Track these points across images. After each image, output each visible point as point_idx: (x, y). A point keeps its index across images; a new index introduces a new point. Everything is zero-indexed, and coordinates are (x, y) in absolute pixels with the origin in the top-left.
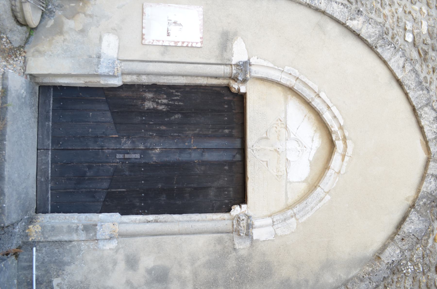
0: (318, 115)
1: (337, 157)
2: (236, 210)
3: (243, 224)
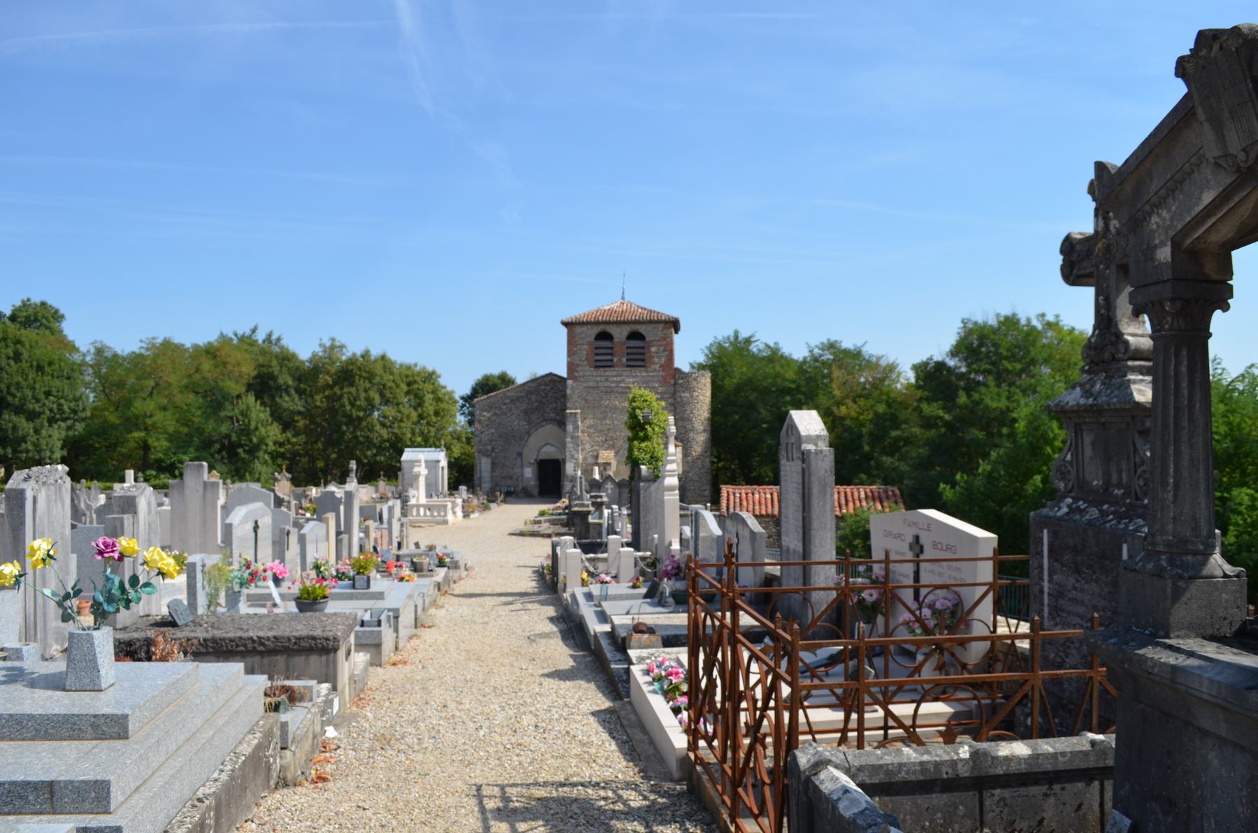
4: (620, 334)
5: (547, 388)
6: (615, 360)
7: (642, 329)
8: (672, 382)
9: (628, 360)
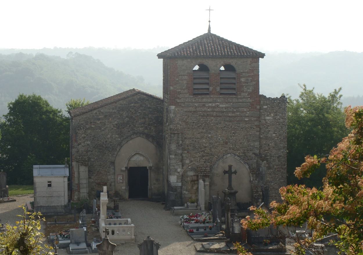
0: (133, 156)
1: (140, 153)
2: (148, 168)
3: (150, 168)
6: (211, 89)
7: (233, 62)
8: (258, 107)
9: (221, 89)
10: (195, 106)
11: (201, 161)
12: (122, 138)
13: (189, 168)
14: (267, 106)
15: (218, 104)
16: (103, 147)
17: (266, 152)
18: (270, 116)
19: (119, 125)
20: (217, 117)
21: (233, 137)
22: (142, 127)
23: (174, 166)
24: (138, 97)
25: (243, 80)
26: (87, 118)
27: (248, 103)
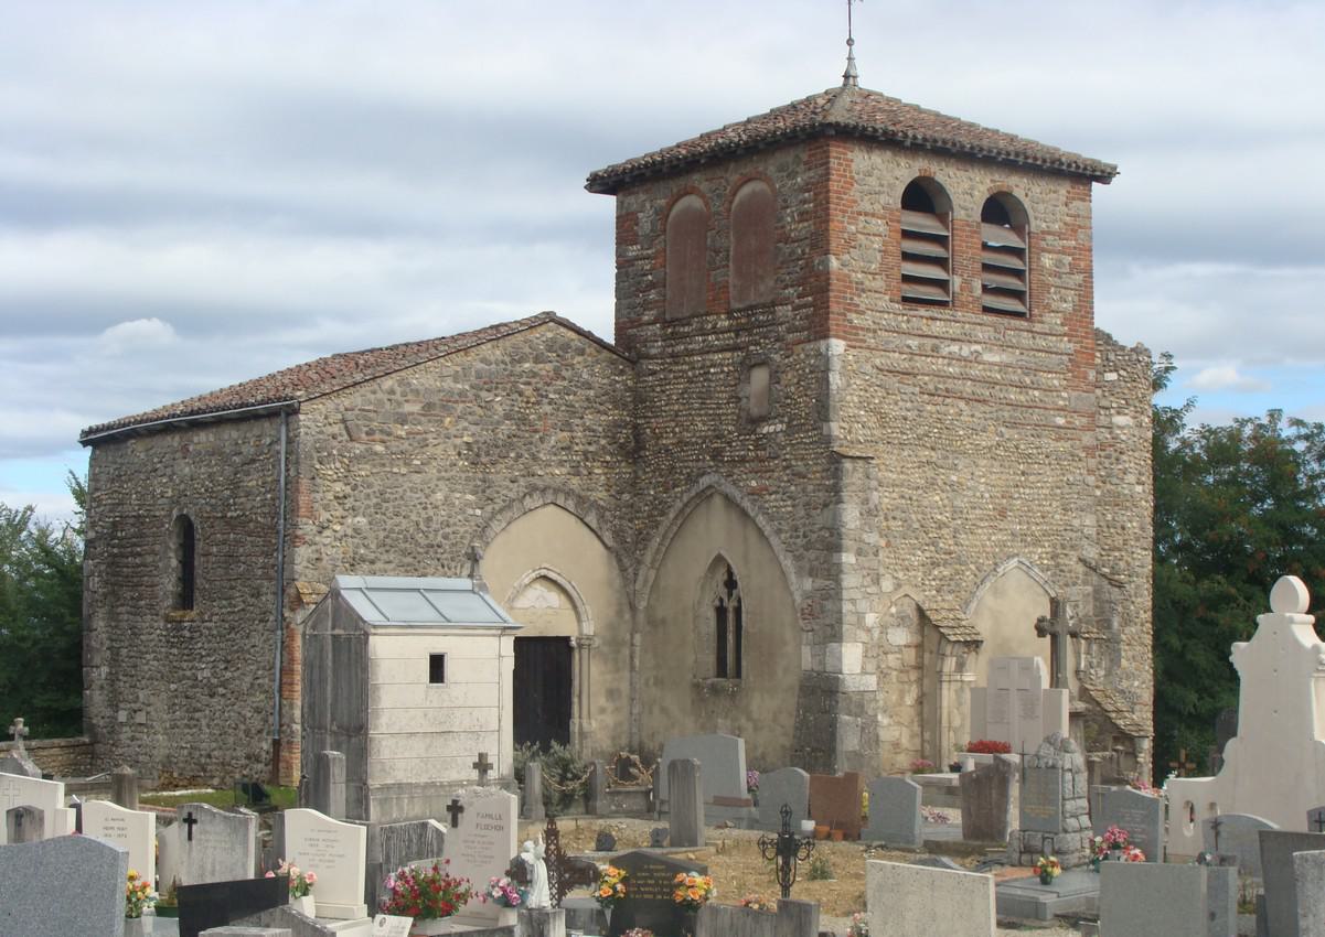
1: (552, 575)
2: (574, 643)
4: (967, 189)
5: (546, 369)
6: (956, 282)
7: (1021, 187)
9: (985, 289)
10: (909, 347)
11: (927, 582)
12: (489, 508)
13: (892, 615)
14: (1117, 371)
15: (978, 347)
16: (418, 544)
17: (1117, 554)
18: (1126, 414)
19: (479, 448)
20: (976, 404)
21: (1022, 490)
22: (561, 463)
23: (853, 601)
24: (550, 335)
25: (1047, 261)
26: (357, 412)
27: (1061, 354)
